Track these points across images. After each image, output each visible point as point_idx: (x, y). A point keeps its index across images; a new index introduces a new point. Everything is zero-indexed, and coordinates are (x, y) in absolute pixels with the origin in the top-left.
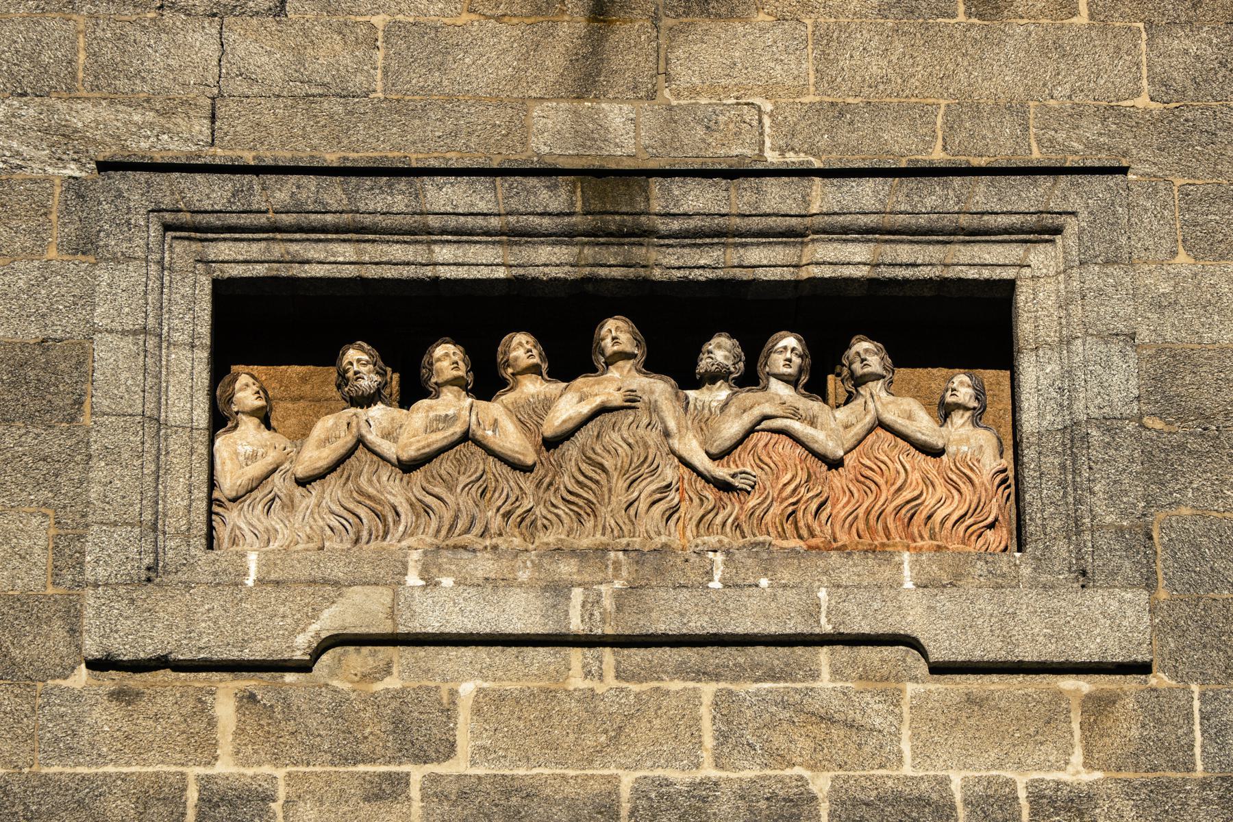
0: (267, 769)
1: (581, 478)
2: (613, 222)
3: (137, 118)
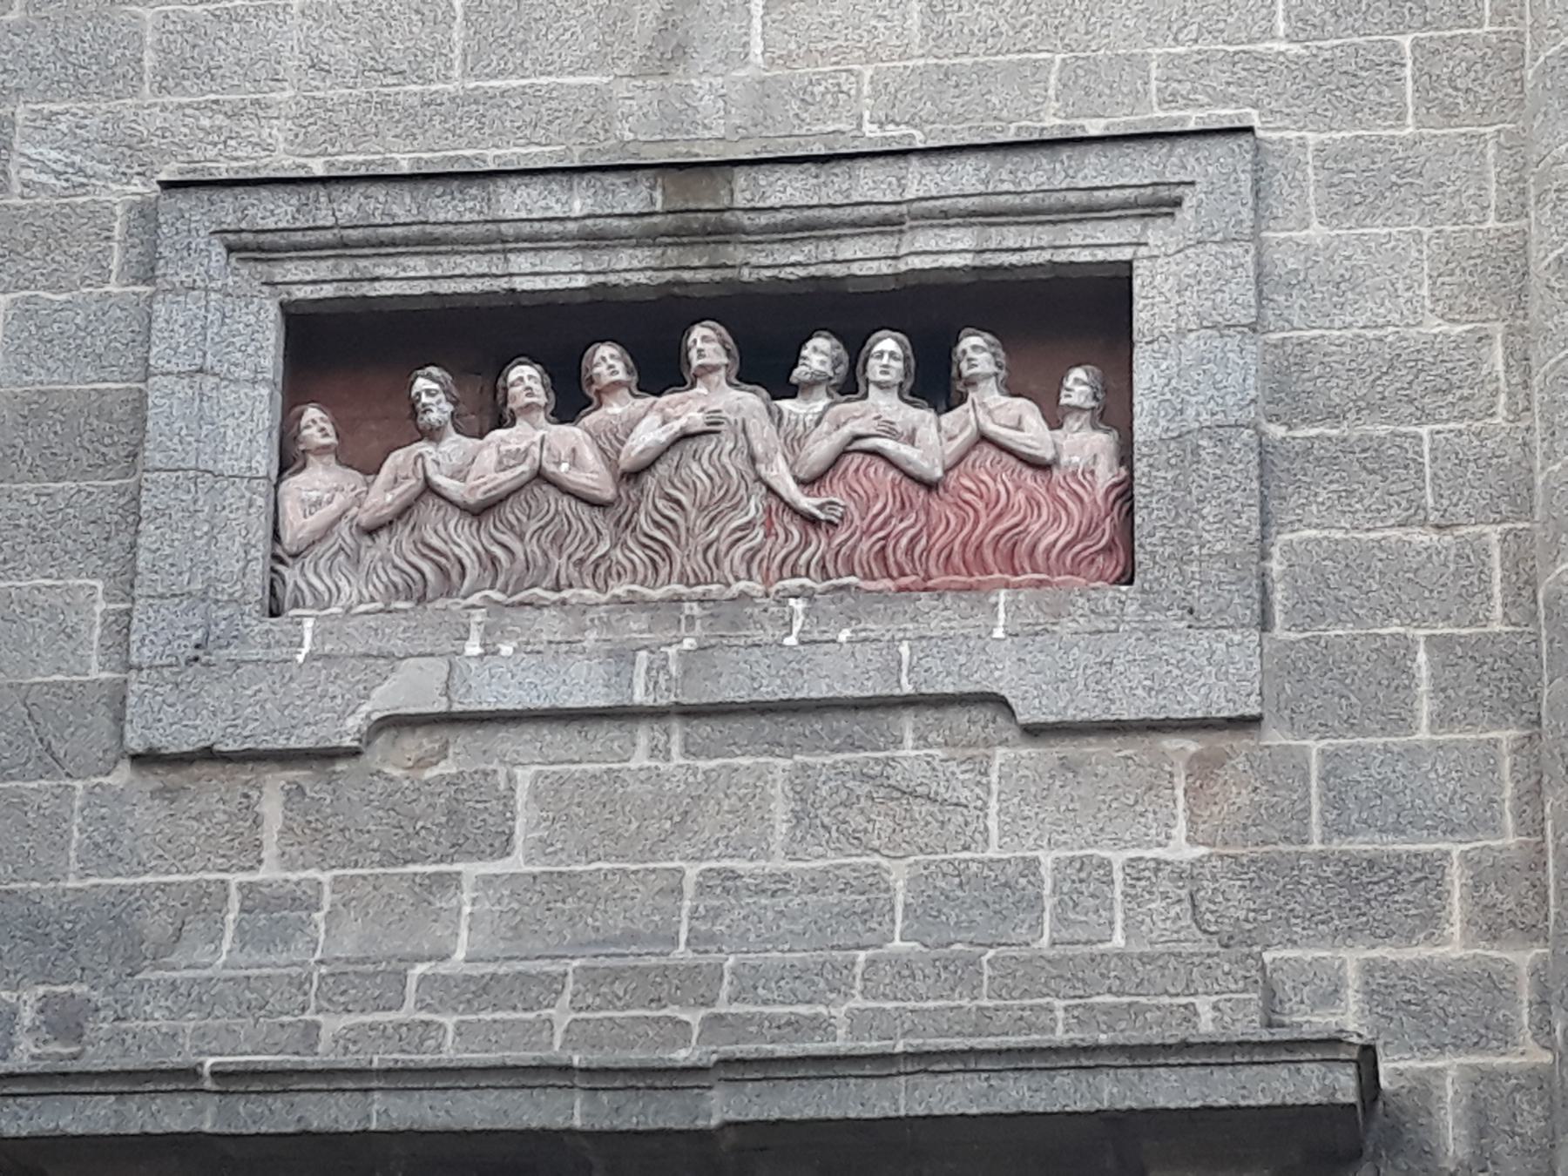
0: (312, 873)
1: (658, 517)
2: (696, 221)
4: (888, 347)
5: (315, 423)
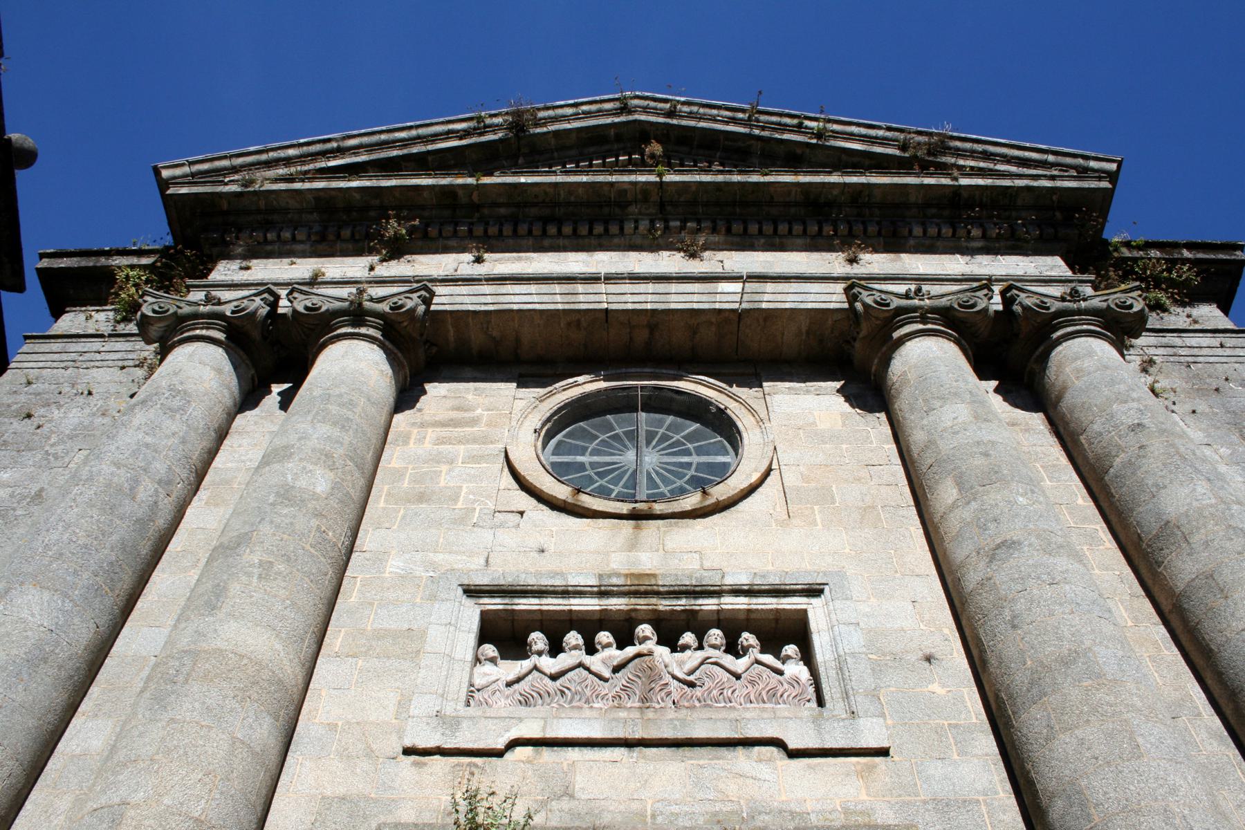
2: (642, 588)
3: (459, 558)
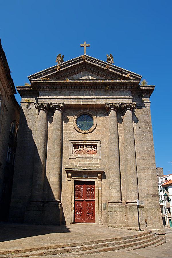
4: (90, 146)
5: (74, 148)
